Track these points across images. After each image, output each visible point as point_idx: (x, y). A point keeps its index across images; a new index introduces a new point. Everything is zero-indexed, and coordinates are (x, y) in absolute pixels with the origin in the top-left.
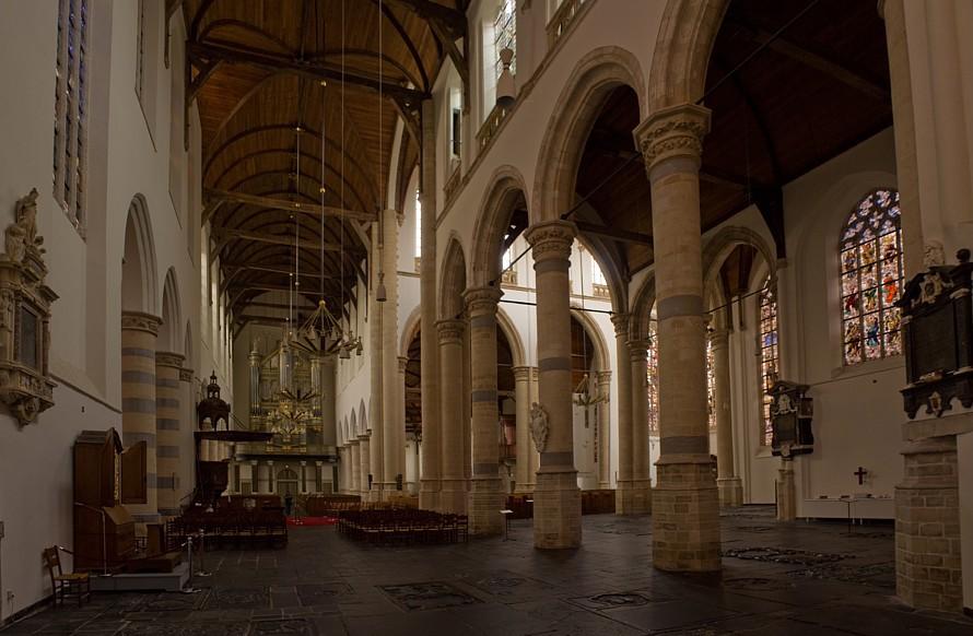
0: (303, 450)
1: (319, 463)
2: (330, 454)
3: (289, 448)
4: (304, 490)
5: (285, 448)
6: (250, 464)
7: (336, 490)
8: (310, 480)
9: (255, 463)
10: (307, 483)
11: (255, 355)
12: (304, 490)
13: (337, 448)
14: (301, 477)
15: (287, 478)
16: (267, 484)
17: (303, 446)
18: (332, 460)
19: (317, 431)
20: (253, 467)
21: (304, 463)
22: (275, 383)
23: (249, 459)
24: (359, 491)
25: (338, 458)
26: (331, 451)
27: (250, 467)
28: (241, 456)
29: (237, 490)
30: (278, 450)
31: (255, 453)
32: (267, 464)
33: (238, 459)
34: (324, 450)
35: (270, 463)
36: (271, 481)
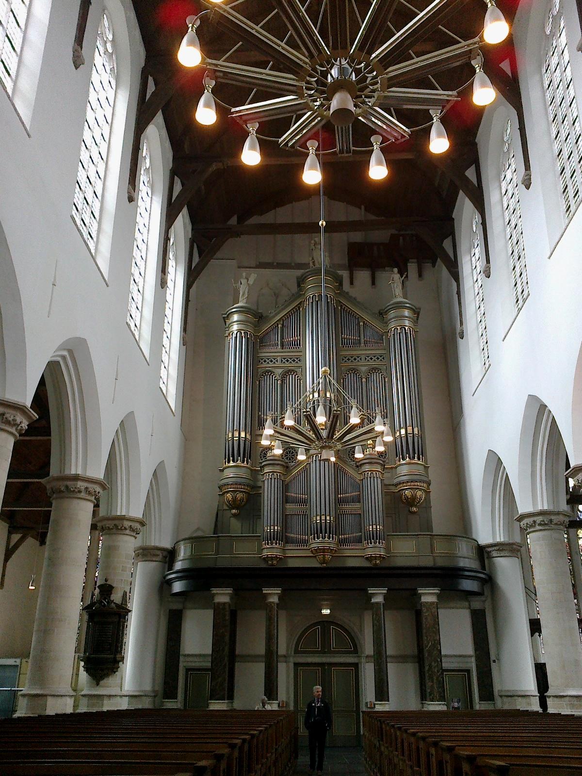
0: (374, 550)
1: (428, 596)
2: (462, 563)
3: (329, 542)
4: (382, 694)
5: (316, 543)
6: (208, 603)
7: (487, 694)
8: (401, 659)
9: (223, 596)
10: (392, 669)
11: (242, 311)
12: (382, 694)
13: (483, 553)
14: (368, 648)
15: (325, 650)
16: (259, 670)
17: (373, 537)
18: (468, 585)
19: (411, 502)
20: (218, 609)
21: (378, 595)
22: (291, 378)
23: (207, 587)
24: (479, 703)
25: (489, 582)
26: (466, 560)
27: (209, 614)
28: (186, 574)
29: (169, 689)
30: (293, 551)
31: (224, 561)
32: (262, 603)
33: (177, 587)
34: (440, 548)
35: (273, 595)
36: (271, 660)
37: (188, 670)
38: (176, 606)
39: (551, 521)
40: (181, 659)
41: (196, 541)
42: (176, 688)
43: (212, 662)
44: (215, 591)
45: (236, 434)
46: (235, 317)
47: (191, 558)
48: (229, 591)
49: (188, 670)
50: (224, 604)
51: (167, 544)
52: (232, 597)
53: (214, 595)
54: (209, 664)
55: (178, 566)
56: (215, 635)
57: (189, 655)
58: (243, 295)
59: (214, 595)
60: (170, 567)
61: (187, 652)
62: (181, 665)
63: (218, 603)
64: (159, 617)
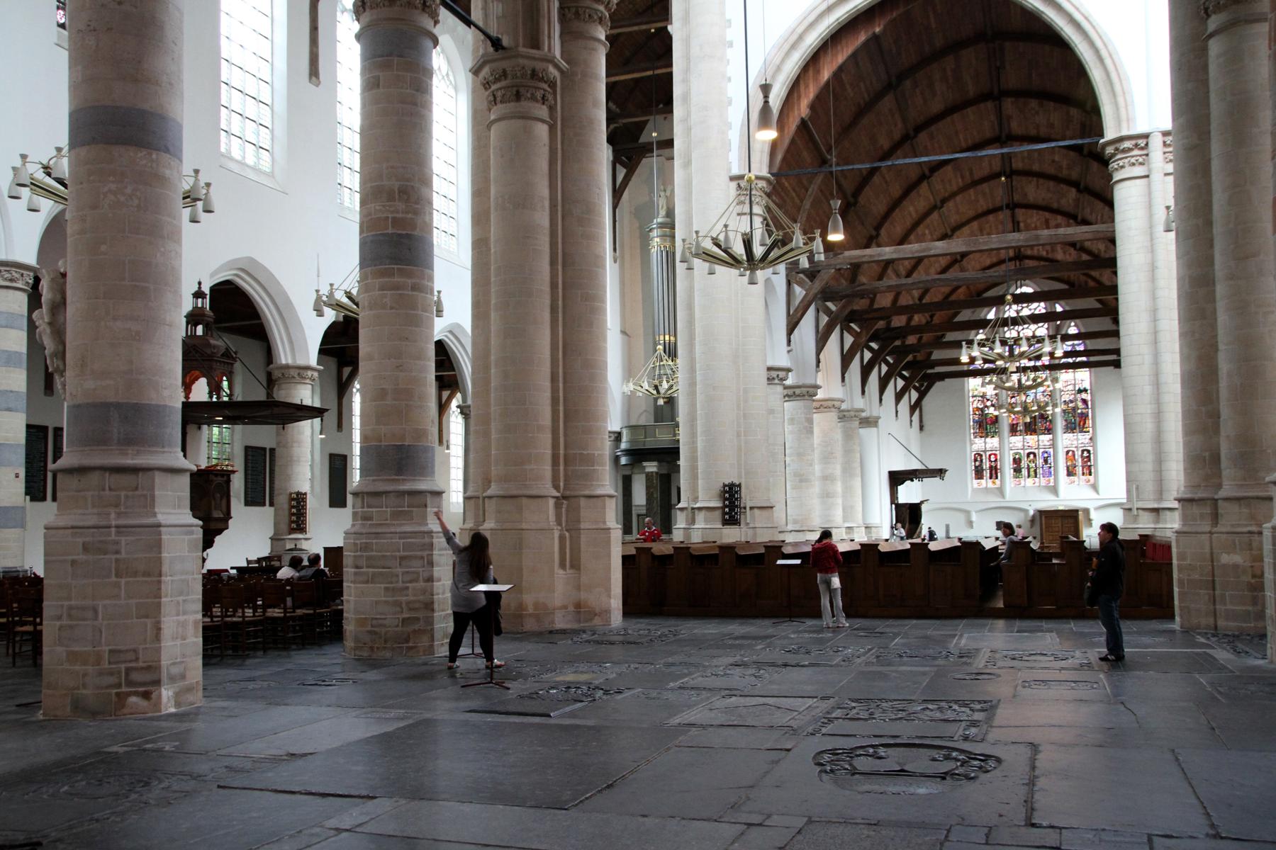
9: (651, 467)
27: (643, 477)
28: (628, 452)
31: (650, 443)
33: (623, 461)
37: (639, 515)
38: (628, 473)
39: (844, 416)
40: (633, 508)
41: (633, 428)
42: (631, 528)
43: (647, 510)
44: (645, 464)
45: (662, 338)
46: (655, 233)
47: (631, 441)
48: (655, 463)
49: (639, 515)
50: (652, 472)
51: (617, 429)
52: (659, 467)
53: (644, 467)
54: (645, 511)
55: (623, 446)
56: (647, 494)
57: (638, 506)
58: (662, 207)
59: (644, 467)
60: (617, 447)
61: (637, 504)
62: (633, 512)
63: (648, 473)
64: (617, 480)
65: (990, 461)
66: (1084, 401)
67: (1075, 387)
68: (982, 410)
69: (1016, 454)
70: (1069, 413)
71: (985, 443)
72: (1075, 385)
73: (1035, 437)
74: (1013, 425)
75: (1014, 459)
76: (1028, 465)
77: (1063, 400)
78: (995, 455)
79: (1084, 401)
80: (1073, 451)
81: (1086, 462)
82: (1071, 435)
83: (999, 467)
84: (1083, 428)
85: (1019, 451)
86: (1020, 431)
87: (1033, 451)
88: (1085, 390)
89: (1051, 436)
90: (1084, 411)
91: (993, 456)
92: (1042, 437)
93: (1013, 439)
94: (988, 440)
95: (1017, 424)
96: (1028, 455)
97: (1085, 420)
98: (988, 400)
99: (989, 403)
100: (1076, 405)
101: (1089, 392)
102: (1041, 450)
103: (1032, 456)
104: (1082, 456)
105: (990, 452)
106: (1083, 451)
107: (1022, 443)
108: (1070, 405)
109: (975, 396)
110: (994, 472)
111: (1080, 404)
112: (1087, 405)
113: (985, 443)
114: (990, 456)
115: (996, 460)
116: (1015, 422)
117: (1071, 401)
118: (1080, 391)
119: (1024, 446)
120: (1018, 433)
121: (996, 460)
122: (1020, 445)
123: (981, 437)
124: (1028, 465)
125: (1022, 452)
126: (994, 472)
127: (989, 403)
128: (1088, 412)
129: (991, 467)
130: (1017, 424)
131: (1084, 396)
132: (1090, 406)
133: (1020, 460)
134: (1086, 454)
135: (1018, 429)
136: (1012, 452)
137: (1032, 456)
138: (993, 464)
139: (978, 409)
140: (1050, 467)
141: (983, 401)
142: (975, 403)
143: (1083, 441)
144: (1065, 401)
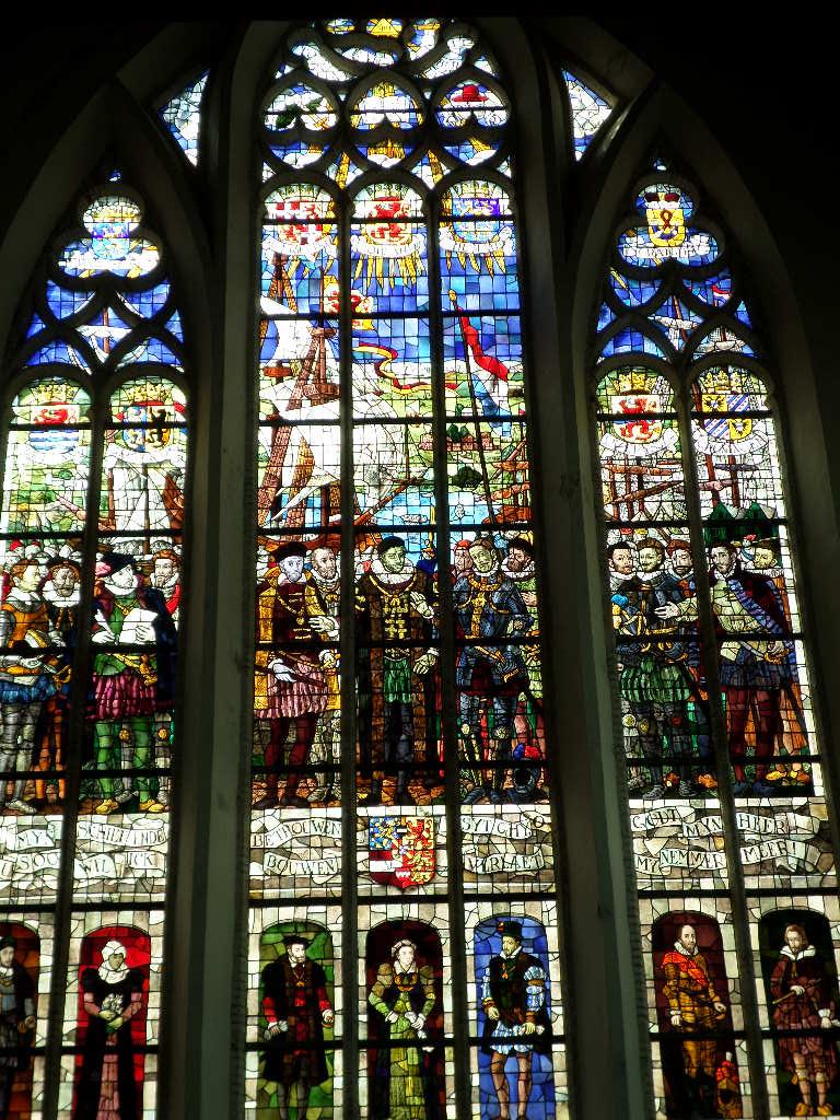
65: (93, 985)
66: (758, 590)
67: (693, 504)
68: (77, 623)
69: (291, 933)
70: (660, 661)
71: (68, 846)
72: (691, 489)
73: (428, 813)
74: (282, 724)
75: (275, 973)
76: (376, 1020)
77: (616, 578)
78: (135, 939)
79: (758, 590)
80: (704, 923)
81: (807, 1006)
82: (684, 807)
83: (152, 1034)
84: (766, 759)
85: (316, 913)
86: (327, 767)
87: (414, 911)
88: (759, 526)
89: (542, 810)
90: (759, 649)
91: (113, 948)
92: (479, 817)
93: (271, 826)
94: (91, 828)
95: (309, 721)
96: (383, 940)
97: (772, 709)
98: (117, 562)
99: (122, 583)
100: (707, 609)
101: (783, 531)
102: (476, 913)
103: (405, 956)
104: (771, 959)
105: (96, 920)
106: (773, 926)
107: (335, 857)
108: (671, 611)
109: (37, 536)
110: (109, 1074)
111: (729, 608)
112: (781, 618)
113: (68, 846)
114: (93, 944)
115: (136, 980)
116: (290, 708)
117: (673, 590)
118: (726, 529)
119: (349, 873)
120: (310, 788)
121: (136, 980)
122: (323, 868)
123: (41, 806)
124: (376, 1020)
125: (333, 917)
126: (109, 1074)
127: (122, 583)
128: (788, 661)
129: (92, 1028)
130: (309, 721)
131: (755, 558)
132: (796, 626)
133: (316, 975)
134: (793, 945)
135: (317, 753)
136: (258, 920)
137: (405, 956)
138: (111, 1011)
139: (42, 612)
140: (543, 1044)
141: (85, 573)
142: (30, 576)
143: (772, 849)
144: (632, 586)
